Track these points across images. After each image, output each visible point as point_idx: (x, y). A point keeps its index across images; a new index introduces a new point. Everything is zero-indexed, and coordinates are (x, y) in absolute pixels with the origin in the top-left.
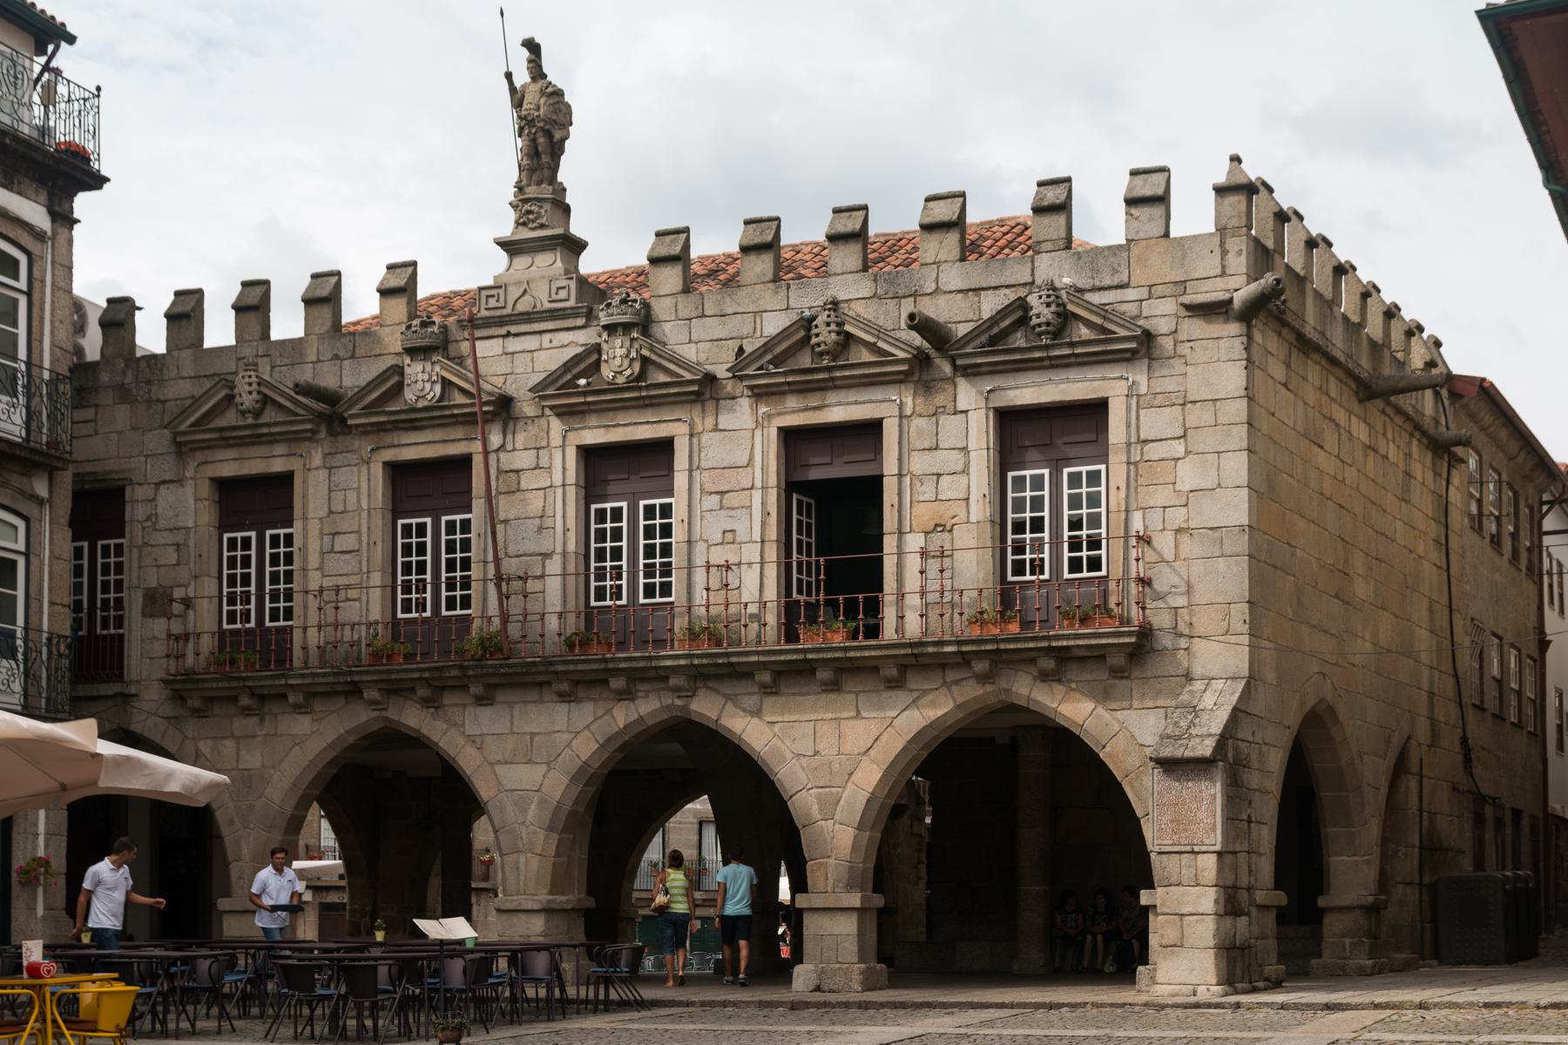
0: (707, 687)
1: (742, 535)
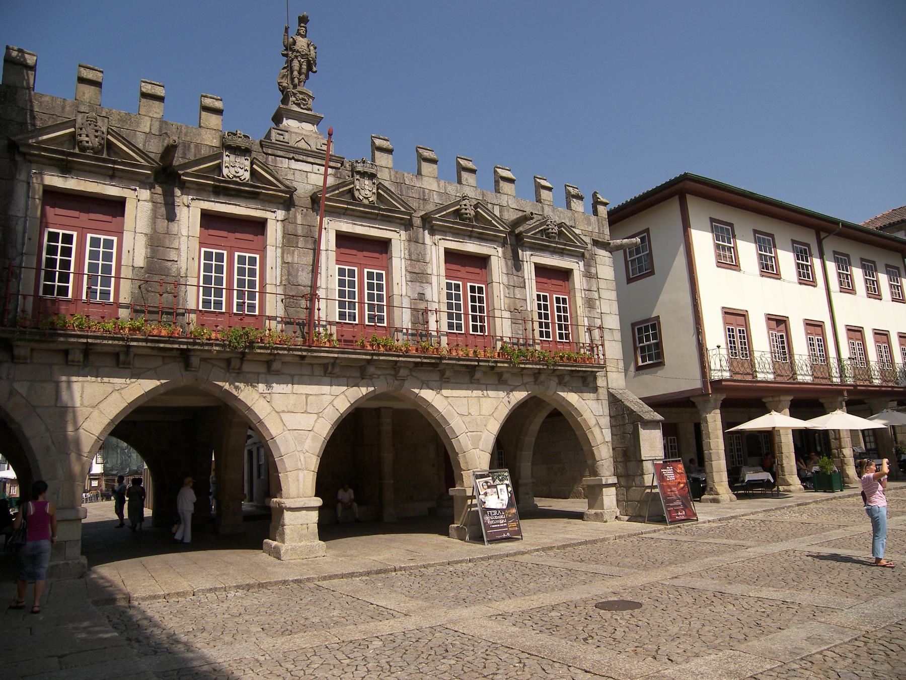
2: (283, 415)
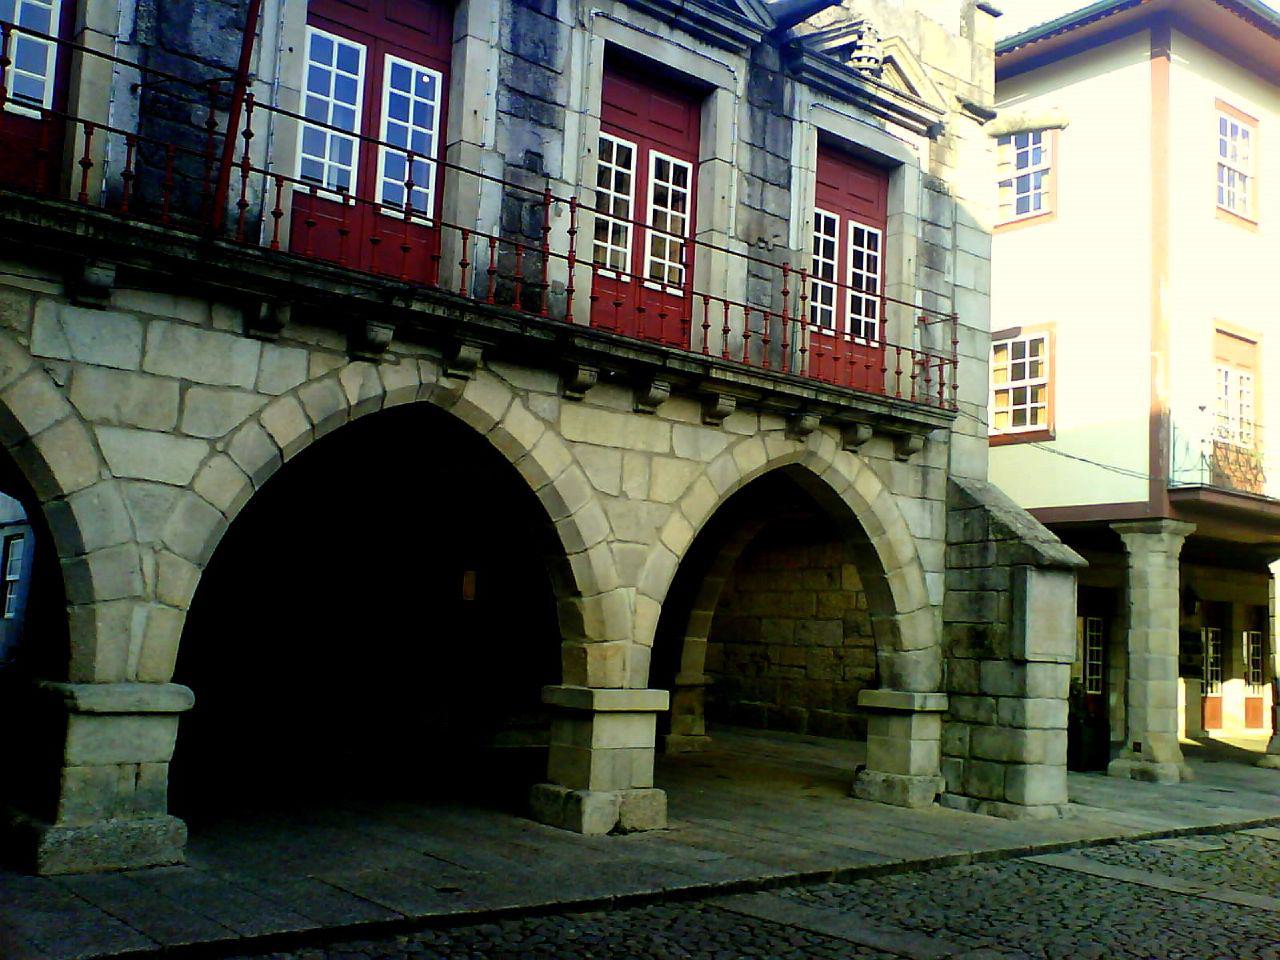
2: (103, 434)
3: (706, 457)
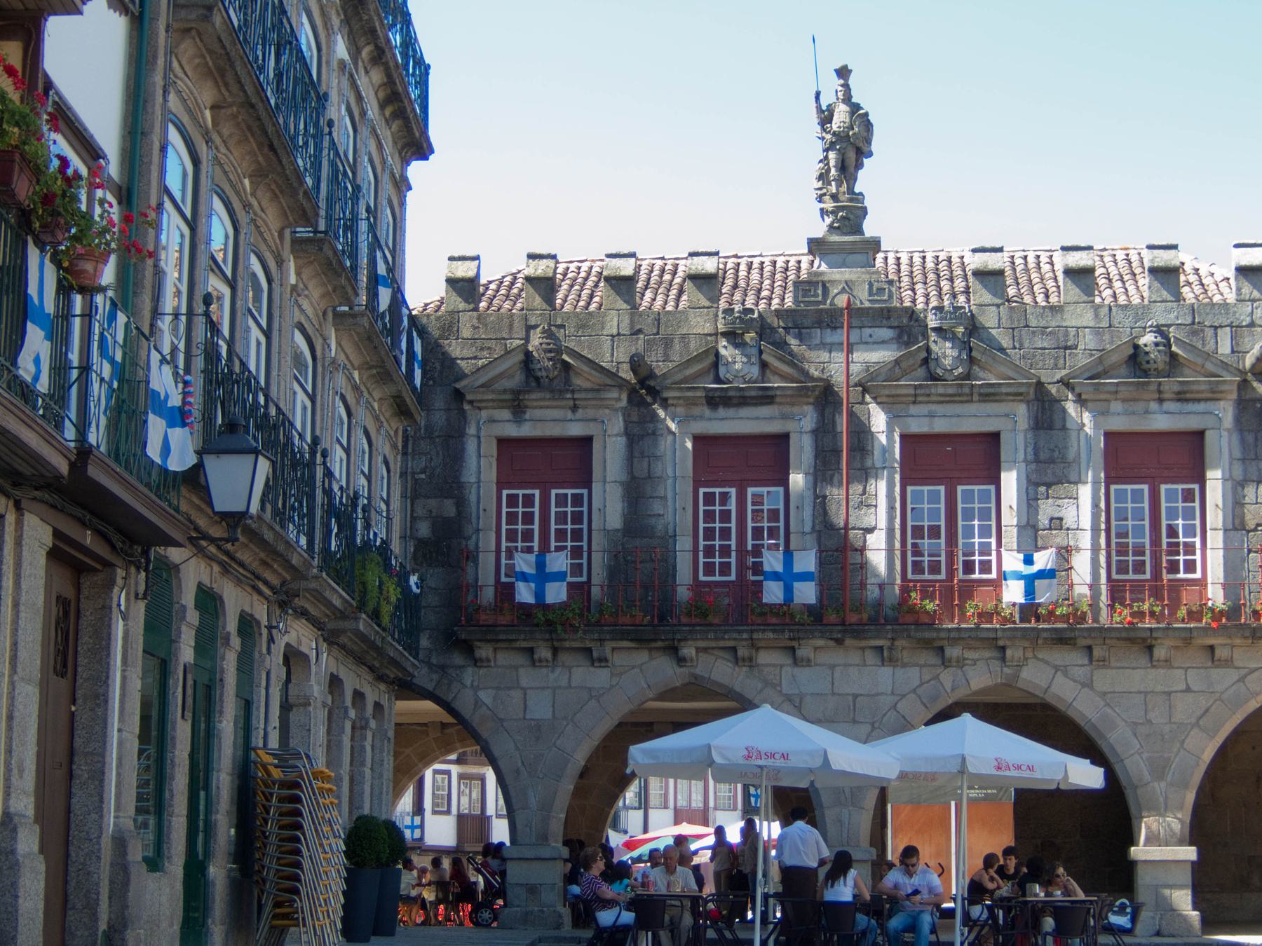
0: (1035, 657)
1: (1069, 521)
3: (1219, 688)
